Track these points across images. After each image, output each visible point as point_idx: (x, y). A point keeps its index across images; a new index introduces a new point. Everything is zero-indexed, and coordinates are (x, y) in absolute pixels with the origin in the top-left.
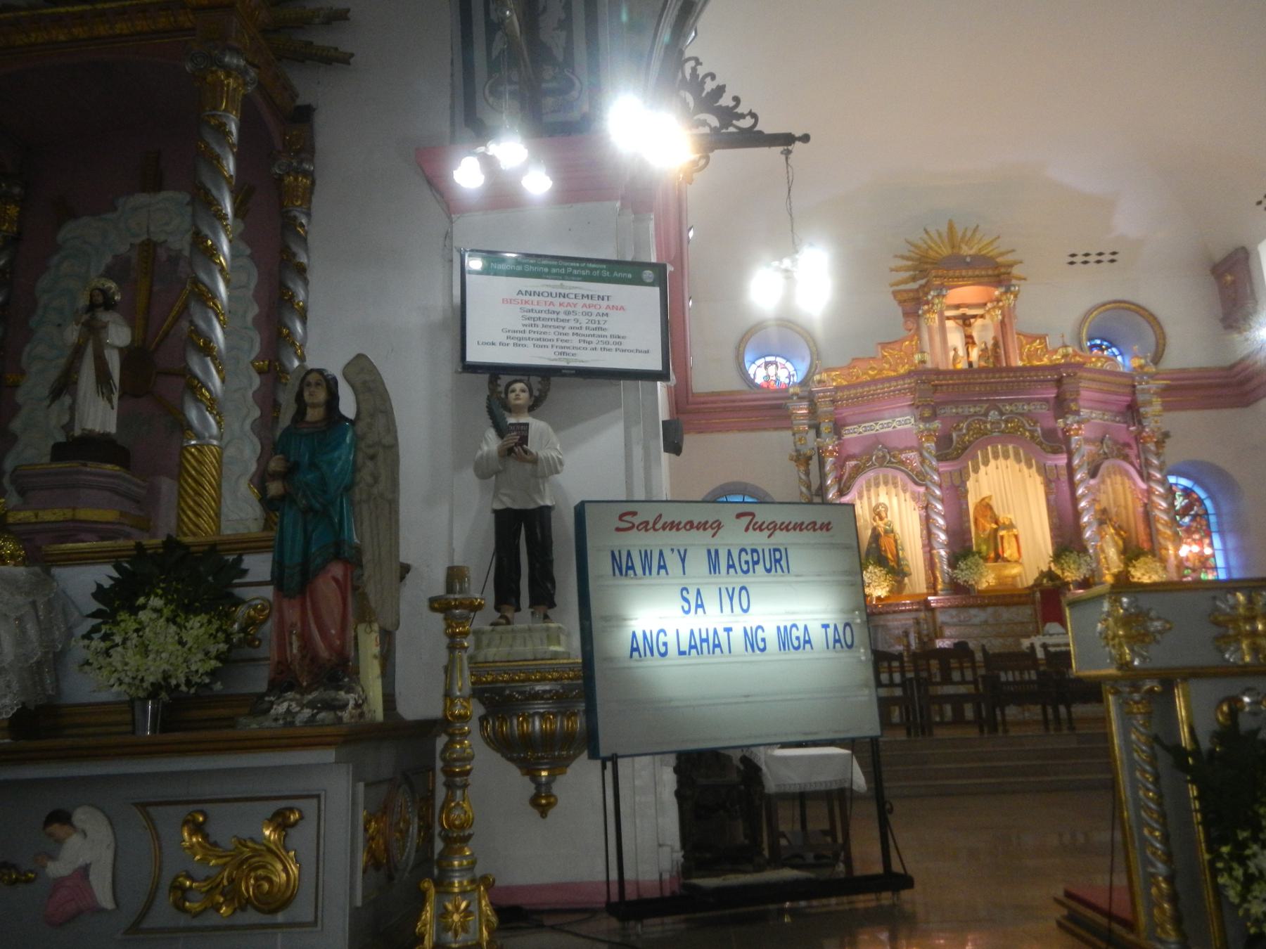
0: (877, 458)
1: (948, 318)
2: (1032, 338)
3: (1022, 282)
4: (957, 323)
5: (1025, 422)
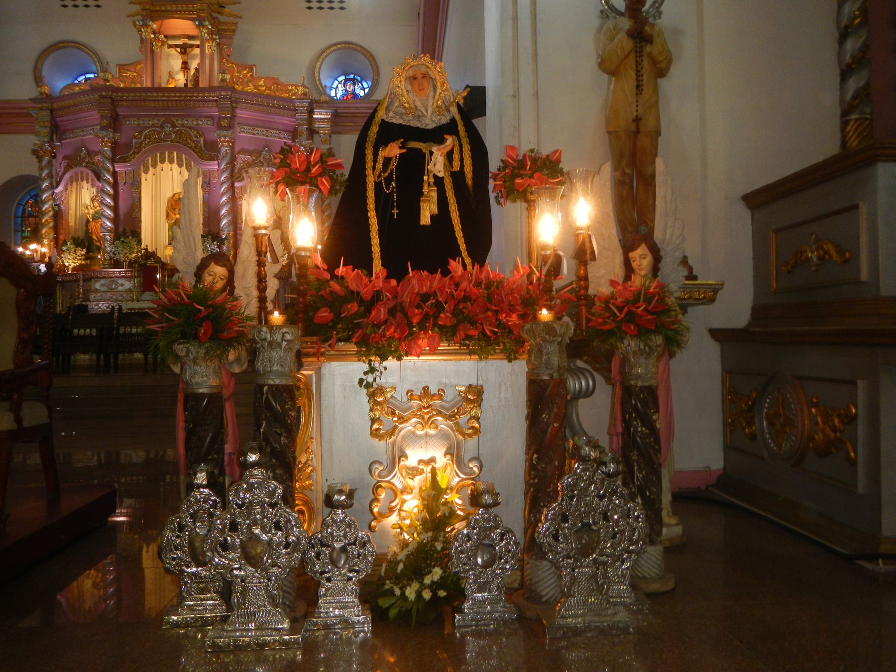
0: (80, 158)
1: (170, 46)
2: (245, 67)
3: (238, 20)
4: (177, 51)
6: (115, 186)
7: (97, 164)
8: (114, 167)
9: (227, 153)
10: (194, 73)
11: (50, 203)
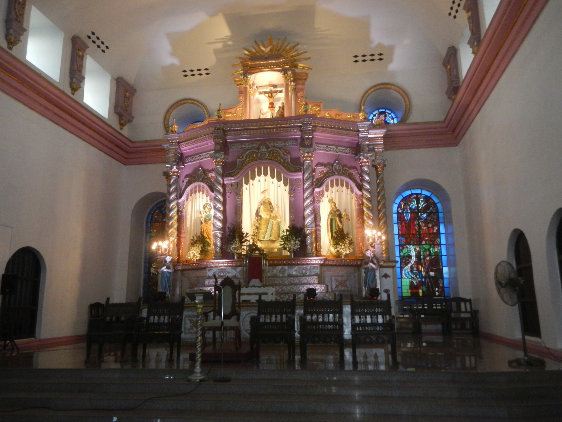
1: (261, 93)
4: (265, 96)
5: (281, 153)
6: (224, 195)
7: (210, 180)
8: (223, 180)
9: (309, 166)
10: (279, 110)
11: (176, 210)
